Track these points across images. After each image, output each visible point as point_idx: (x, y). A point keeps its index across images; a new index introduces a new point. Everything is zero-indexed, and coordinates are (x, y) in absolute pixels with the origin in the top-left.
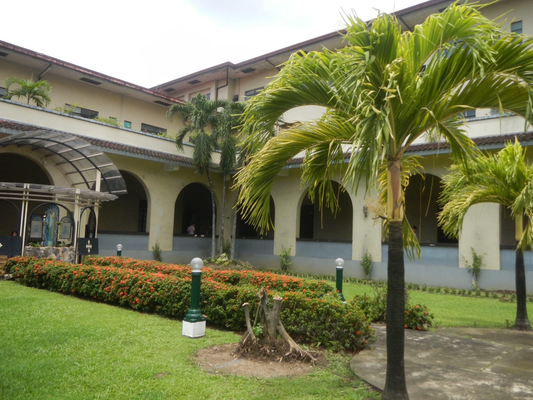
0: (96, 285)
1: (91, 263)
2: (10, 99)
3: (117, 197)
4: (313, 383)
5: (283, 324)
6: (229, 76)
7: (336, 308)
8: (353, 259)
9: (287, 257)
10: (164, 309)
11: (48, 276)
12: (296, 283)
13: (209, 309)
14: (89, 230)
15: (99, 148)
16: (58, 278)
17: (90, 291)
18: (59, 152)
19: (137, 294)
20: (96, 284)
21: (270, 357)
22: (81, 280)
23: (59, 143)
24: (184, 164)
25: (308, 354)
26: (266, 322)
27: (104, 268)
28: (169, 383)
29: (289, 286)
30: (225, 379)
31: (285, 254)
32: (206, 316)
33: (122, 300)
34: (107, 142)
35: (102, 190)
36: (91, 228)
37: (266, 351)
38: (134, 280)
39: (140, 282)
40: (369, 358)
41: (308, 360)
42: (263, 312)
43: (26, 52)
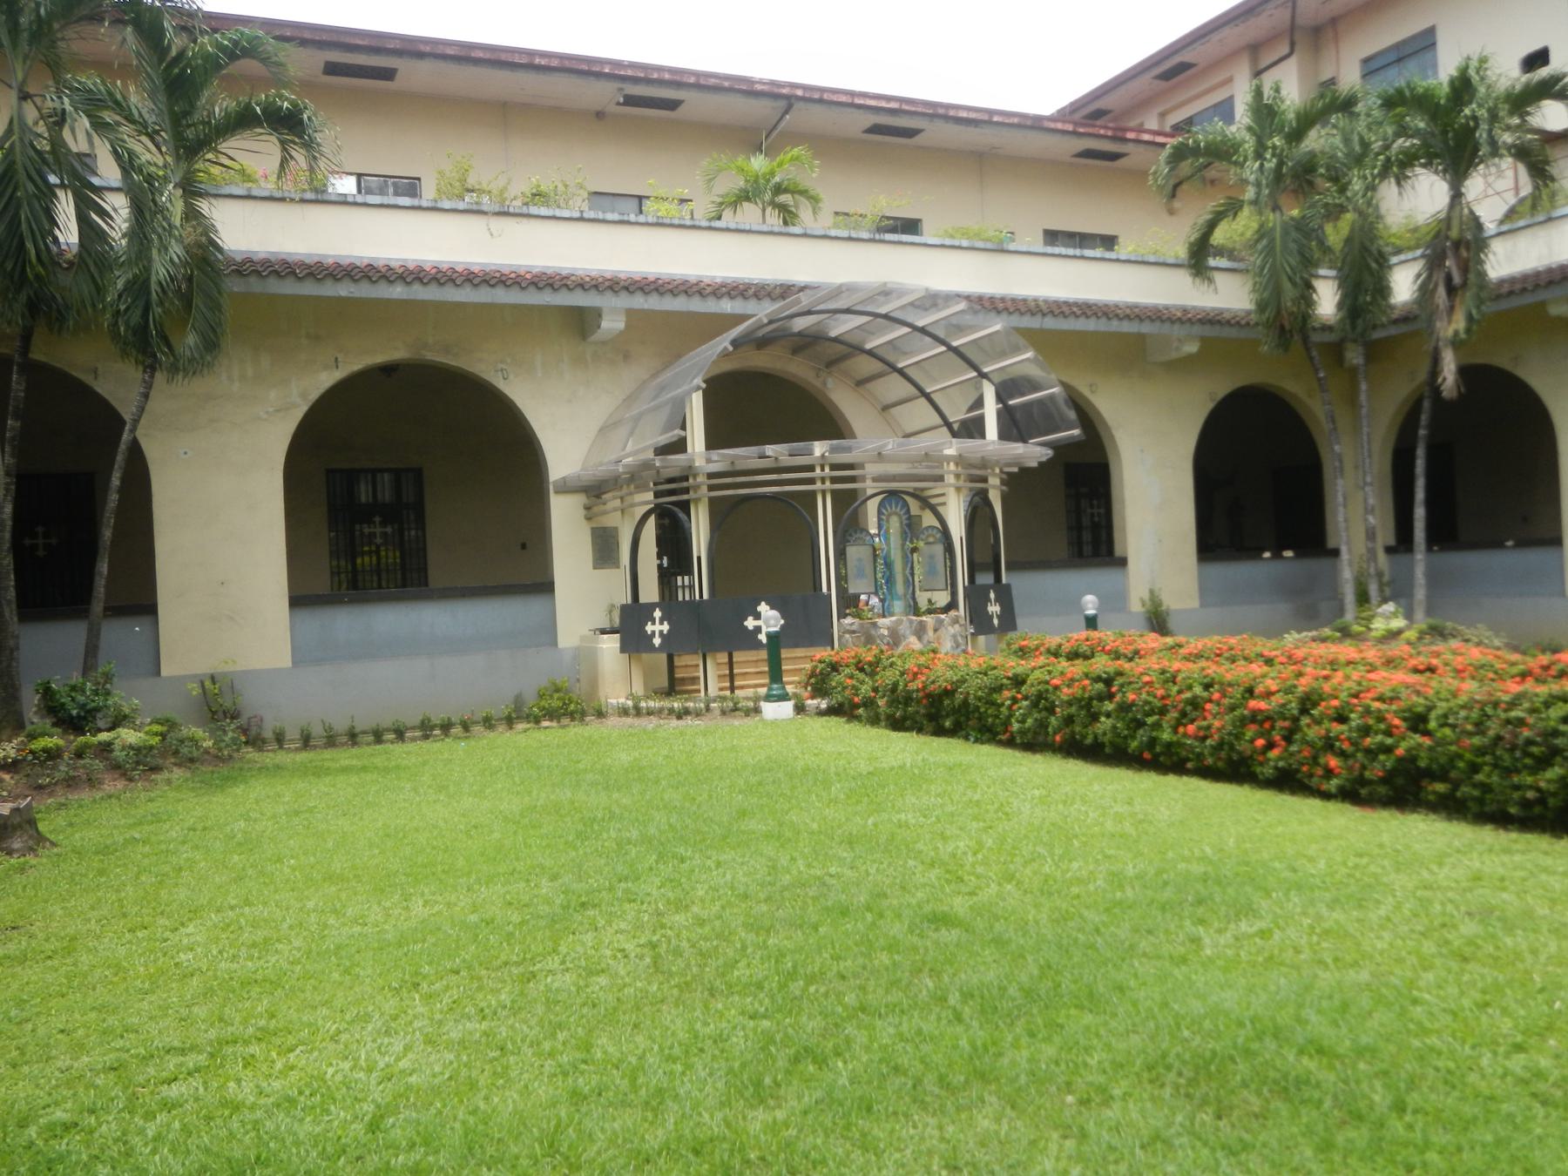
0: (1150, 720)
2: (719, 218)
6: (1299, 21)
10: (1465, 790)
11: (959, 697)
16: (993, 703)
17: (1125, 737)
18: (868, 346)
19: (1329, 744)
20: (1148, 715)
24: (1218, 327)
35: (1004, 435)
39: (1336, 703)
43: (726, 84)
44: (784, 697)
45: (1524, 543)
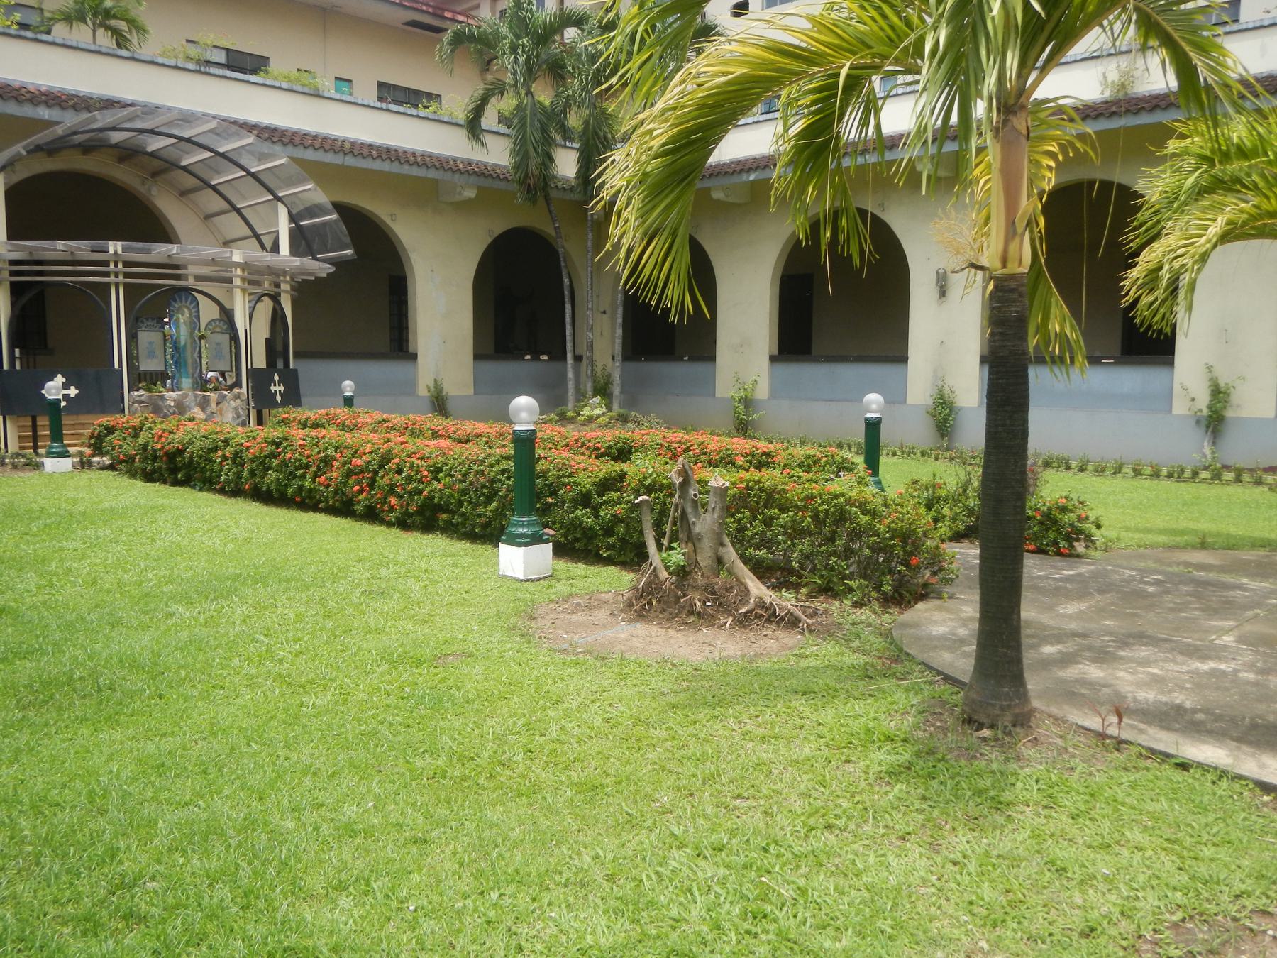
0: (298, 473)
1: (284, 422)
2: (48, 32)
3: (332, 269)
4: (804, 670)
5: (733, 544)
7: (861, 504)
8: (909, 400)
9: (747, 402)
10: (457, 519)
11: (187, 455)
12: (768, 454)
13: (559, 518)
14: (275, 349)
15: (278, 148)
16: (211, 461)
17: (286, 486)
18: (183, 163)
19: (391, 489)
20: (298, 469)
21: (703, 618)
22: (263, 463)
23: (181, 139)
25: (793, 609)
26: (692, 539)
27: (313, 433)
28: (469, 674)
29: (750, 462)
30: (598, 664)
31: (742, 393)
32: (552, 532)
33: (359, 502)
34: (295, 133)
35: (295, 251)
36: (279, 347)
37: (692, 605)
38: (383, 458)
39: (397, 460)
40: (937, 616)
41: (792, 623)
42: (684, 514)
44: (65, 454)
45: (692, 359)
